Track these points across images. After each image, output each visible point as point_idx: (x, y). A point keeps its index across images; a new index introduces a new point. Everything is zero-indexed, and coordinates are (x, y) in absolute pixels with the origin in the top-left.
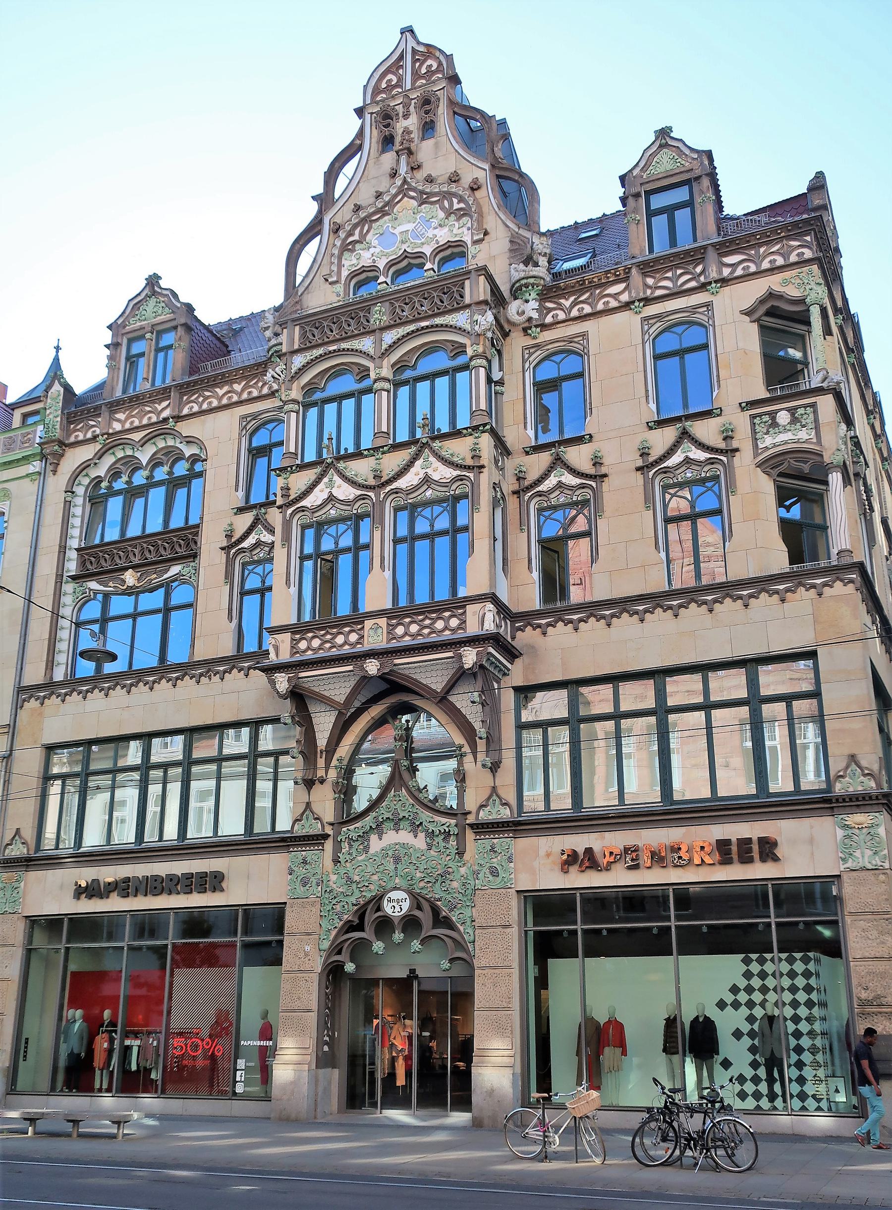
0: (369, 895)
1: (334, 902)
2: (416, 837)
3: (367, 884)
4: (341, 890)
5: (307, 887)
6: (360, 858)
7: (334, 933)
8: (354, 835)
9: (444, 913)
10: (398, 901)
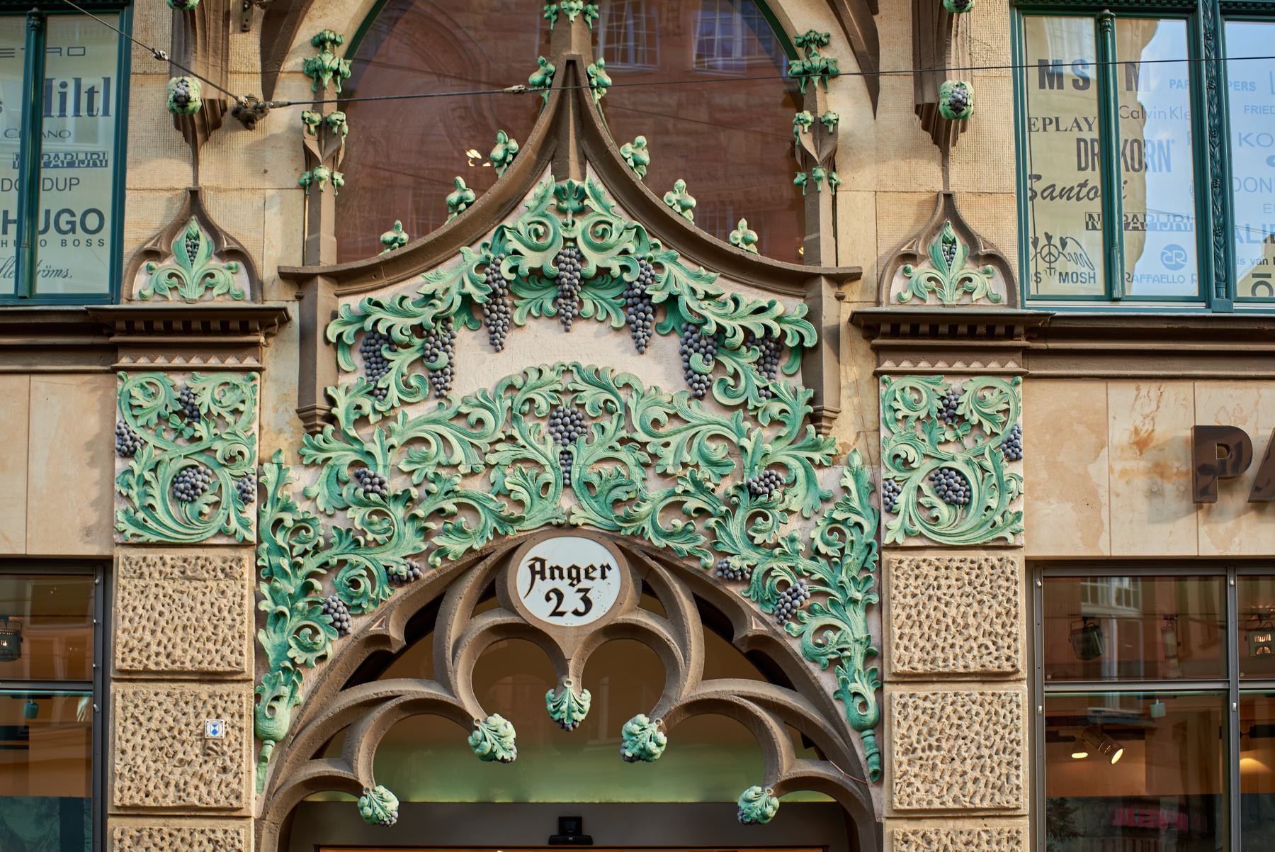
0: (456, 547)
1: (310, 564)
2: (640, 348)
3: (450, 506)
4: (340, 521)
5: (202, 504)
6: (413, 413)
7: (311, 677)
8: (400, 326)
9: (756, 627)
10: (575, 574)
